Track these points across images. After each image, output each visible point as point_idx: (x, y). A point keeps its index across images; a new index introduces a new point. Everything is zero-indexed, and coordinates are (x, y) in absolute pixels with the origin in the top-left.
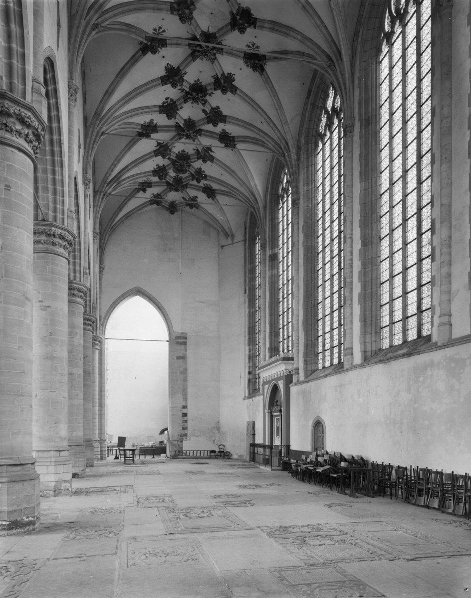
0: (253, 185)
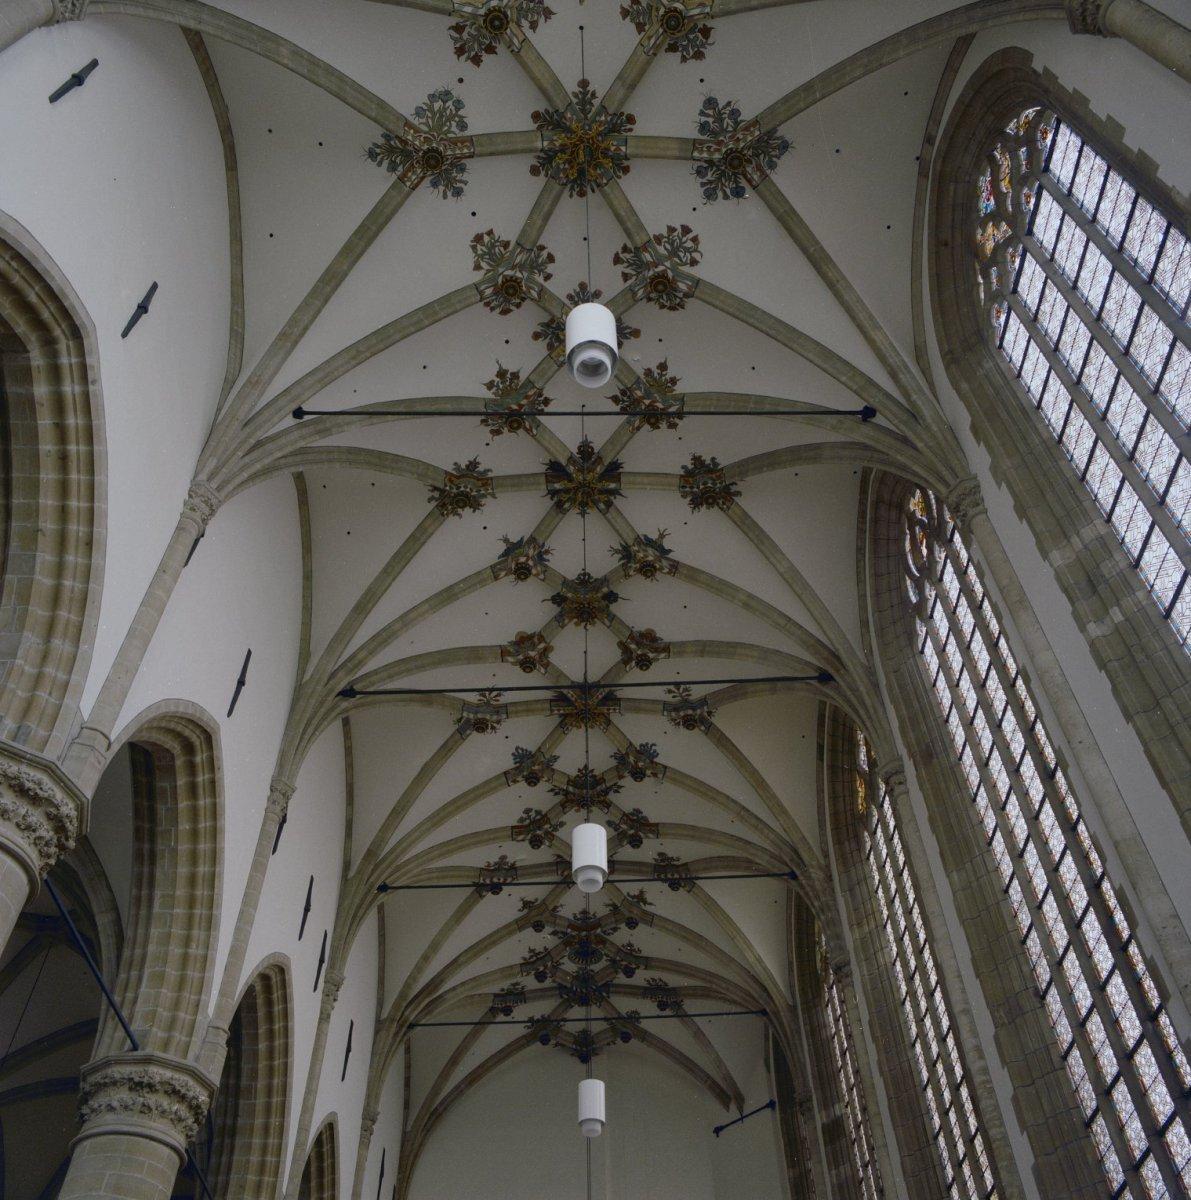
0: (752, 959)
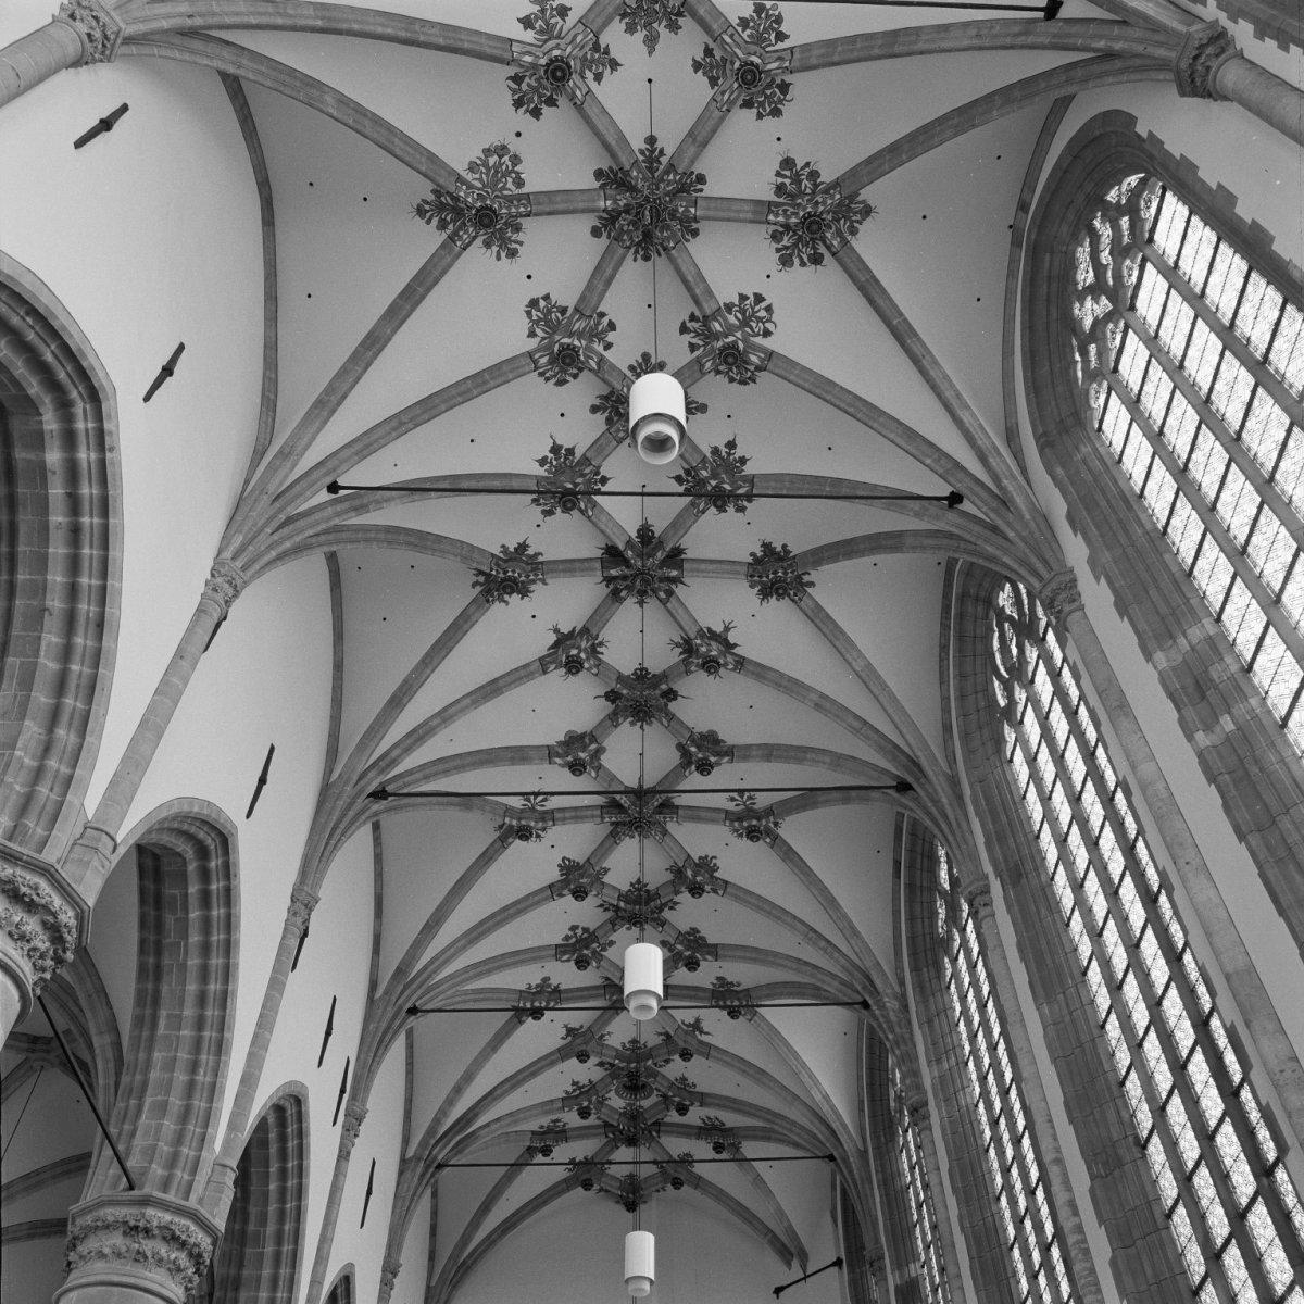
0: (818, 1097)
